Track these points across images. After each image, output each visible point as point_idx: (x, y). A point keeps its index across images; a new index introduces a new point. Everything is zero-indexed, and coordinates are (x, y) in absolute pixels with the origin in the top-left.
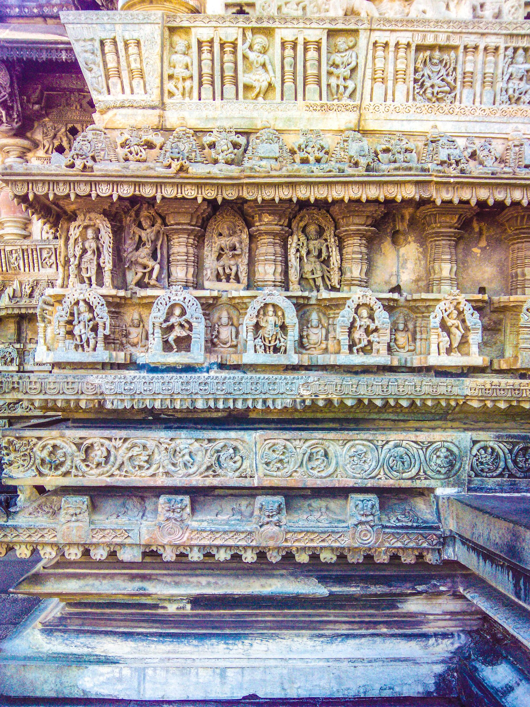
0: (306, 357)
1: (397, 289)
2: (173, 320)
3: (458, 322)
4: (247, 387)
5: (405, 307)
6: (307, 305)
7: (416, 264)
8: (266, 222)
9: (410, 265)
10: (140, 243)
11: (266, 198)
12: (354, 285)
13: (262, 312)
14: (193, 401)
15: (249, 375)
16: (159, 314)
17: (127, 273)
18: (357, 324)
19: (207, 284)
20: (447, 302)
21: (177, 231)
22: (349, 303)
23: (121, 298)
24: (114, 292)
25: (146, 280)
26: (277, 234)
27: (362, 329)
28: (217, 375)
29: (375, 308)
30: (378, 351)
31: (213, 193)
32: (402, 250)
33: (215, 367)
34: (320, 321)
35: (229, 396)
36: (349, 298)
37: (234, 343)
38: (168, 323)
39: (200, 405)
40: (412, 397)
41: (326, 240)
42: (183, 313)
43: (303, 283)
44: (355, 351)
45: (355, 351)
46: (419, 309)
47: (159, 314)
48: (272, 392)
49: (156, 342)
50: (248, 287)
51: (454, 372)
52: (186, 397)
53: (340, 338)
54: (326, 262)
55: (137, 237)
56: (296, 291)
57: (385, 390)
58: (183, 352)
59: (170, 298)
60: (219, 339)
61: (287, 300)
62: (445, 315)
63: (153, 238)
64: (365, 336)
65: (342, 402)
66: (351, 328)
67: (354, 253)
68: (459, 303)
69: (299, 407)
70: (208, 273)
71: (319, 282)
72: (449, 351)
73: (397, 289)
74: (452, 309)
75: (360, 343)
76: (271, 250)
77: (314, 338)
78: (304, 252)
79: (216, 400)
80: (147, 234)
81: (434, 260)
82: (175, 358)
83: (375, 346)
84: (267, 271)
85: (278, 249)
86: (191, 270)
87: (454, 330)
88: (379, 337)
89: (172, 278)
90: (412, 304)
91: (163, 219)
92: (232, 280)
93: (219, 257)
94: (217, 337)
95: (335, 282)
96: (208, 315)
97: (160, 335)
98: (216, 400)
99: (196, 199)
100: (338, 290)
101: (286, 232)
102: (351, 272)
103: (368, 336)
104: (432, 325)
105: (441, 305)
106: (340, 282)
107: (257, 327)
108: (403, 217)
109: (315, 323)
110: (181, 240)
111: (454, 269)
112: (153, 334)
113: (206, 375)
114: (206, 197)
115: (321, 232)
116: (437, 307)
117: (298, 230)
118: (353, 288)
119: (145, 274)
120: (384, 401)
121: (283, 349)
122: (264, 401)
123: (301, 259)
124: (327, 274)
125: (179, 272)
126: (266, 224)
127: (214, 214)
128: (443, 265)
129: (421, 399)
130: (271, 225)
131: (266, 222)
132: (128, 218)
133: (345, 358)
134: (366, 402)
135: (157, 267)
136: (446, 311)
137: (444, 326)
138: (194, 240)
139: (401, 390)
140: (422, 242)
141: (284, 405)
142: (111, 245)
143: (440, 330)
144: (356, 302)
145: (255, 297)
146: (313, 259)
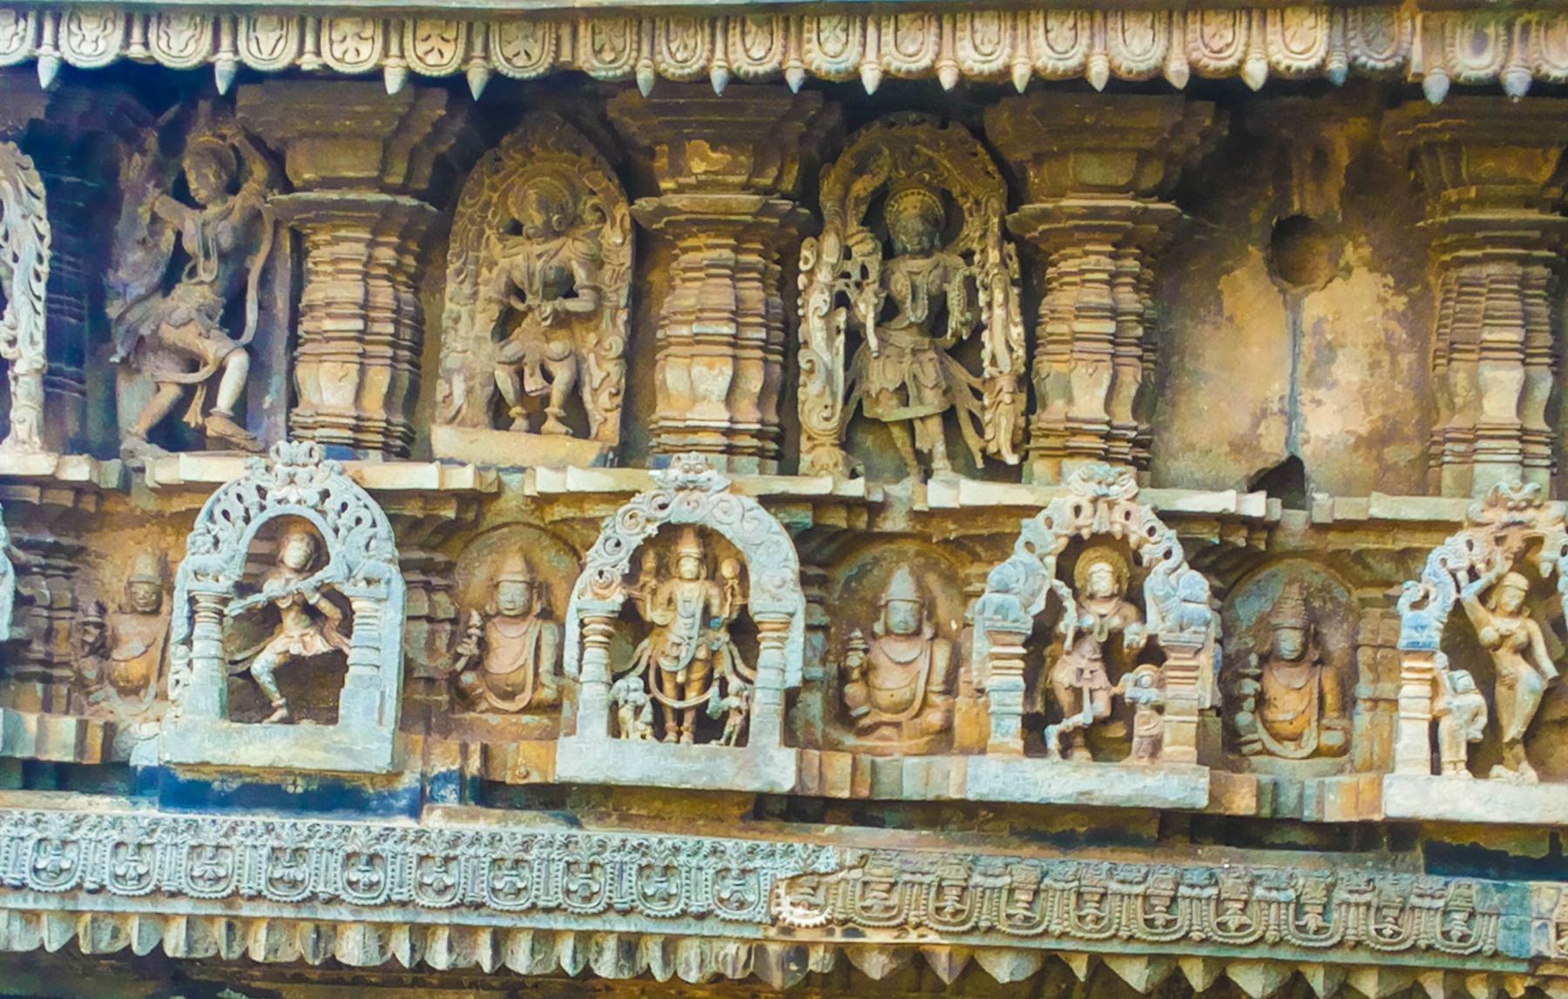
0: (840, 765)
1: (1285, 479)
2: (273, 587)
3: (1528, 629)
4: (547, 883)
5: (1310, 555)
6: (872, 537)
7: (1374, 365)
8: (702, 178)
9: (1348, 372)
10: (177, 267)
11: (672, 70)
12: (1074, 453)
13: (650, 562)
14: (326, 932)
15: (594, 831)
16: (214, 560)
17: (123, 386)
18: (1067, 625)
19: (443, 438)
20: (1478, 535)
21: (327, 214)
22: (1031, 528)
23: (79, 489)
24: (41, 463)
25: (193, 417)
26: (747, 227)
27: (1089, 648)
28: (456, 826)
29: (1147, 553)
30: (1156, 745)
31: (448, 50)
32: (1315, 305)
33: (450, 793)
34: (926, 607)
35: (473, 919)
36: (1031, 511)
37: (547, 694)
38: (252, 599)
39: (353, 950)
40: (1283, 954)
41: (968, 256)
42: (318, 557)
43: (868, 440)
44: (1053, 743)
45: (1053, 743)
46: (1371, 563)
47: (214, 560)
48: (657, 908)
49: (197, 675)
50: (626, 453)
51: (1515, 851)
52: (289, 913)
53: (990, 683)
54: (966, 350)
55: (169, 236)
56: (822, 475)
57: (1161, 919)
58: (307, 725)
59: (262, 492)
60: (485, 673)
61: (761, 512)
62: (1470, 593)
63: (226, 241)
64: (1101, 679)
65: (971, 968)
66: (1041, 642)
67: (1082, 311)
68: (1535, 542)
69: (777, 980)
70: (455, 390)
71: (932, 437)
72: (1480, 758)
73: (1285, 479)
74: (1502, 564)
75: (1078, 707)
76: (720, 294)
77: (892, 683)
78: (866, 310)
79: (421, 934)
80: (206, 225)
81: (1452, 348)
82: (271, 747)
83: (1144, 726)
84: (700, 386)
85: (753, 293)
86: (380, 378)
87: (1508, 662)
88: (1160, 684)
89: (302, 413)
90: (1336, 541)
91: (276, 159)
92: (551, 424)
93: (506, 323)
94: (476, 664)
95: (1000, 439)
96: (448, 569)
97: (214, 649)
98: (421, 934)
99: (377, 75)
100: (1013, 475)
101: (787, 218)
102: (1070, 400)
103: (1114, 678)
104: (1406, 637)
105: (1453, 551)
106: (1022, 440)
107: (630, 623)
108: (1321, 160)
109: (901, 612)
110: (343, 249)
111: (1544, 389)
112: (188, 641)
113: (402, 823)
114: (419, 68)
115: (944, 229)
116: (1434, 557)
117: (842, 213)
118: (1067, 464)
119: (189, 391)
120: (1162, 971)
121: (735, 721)
122: (629, 946)
123: (854, 337)
124: (966, 403)
125: (329, 388)
126: (700, 186)
127: (494, 143)
128: (1488, 372)
129: (1330, 967)
130: (726, 187)
131: (702, 178)
132: (137, 157)
133: (1004, 774)
134: (1080, 969)
135: (237, 364)
136: (1473, 574)
137: (1464, 645)
138: (401, 250)
139: (1233, 921)
140: (1407, 264)
141: (712, 968)
142: (44, 269)
143: (1442, 659)
144: (1066, 524)
145: (627, 495)
146: (906, 340)
